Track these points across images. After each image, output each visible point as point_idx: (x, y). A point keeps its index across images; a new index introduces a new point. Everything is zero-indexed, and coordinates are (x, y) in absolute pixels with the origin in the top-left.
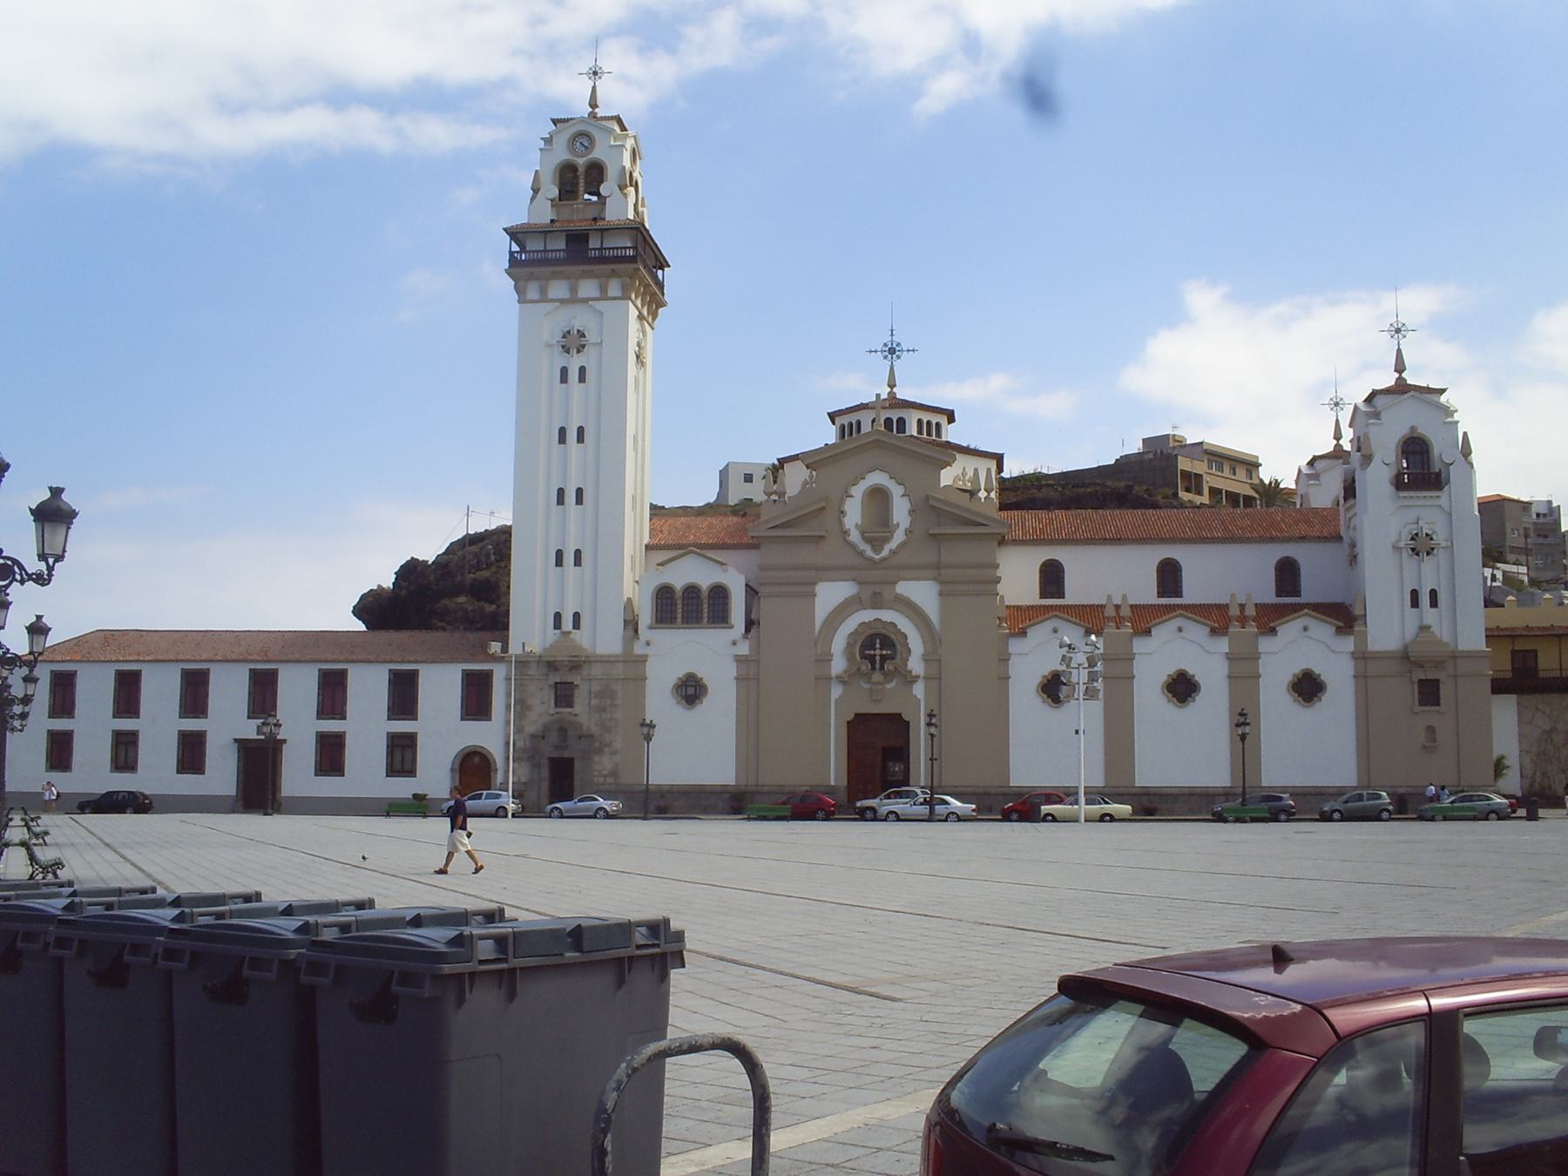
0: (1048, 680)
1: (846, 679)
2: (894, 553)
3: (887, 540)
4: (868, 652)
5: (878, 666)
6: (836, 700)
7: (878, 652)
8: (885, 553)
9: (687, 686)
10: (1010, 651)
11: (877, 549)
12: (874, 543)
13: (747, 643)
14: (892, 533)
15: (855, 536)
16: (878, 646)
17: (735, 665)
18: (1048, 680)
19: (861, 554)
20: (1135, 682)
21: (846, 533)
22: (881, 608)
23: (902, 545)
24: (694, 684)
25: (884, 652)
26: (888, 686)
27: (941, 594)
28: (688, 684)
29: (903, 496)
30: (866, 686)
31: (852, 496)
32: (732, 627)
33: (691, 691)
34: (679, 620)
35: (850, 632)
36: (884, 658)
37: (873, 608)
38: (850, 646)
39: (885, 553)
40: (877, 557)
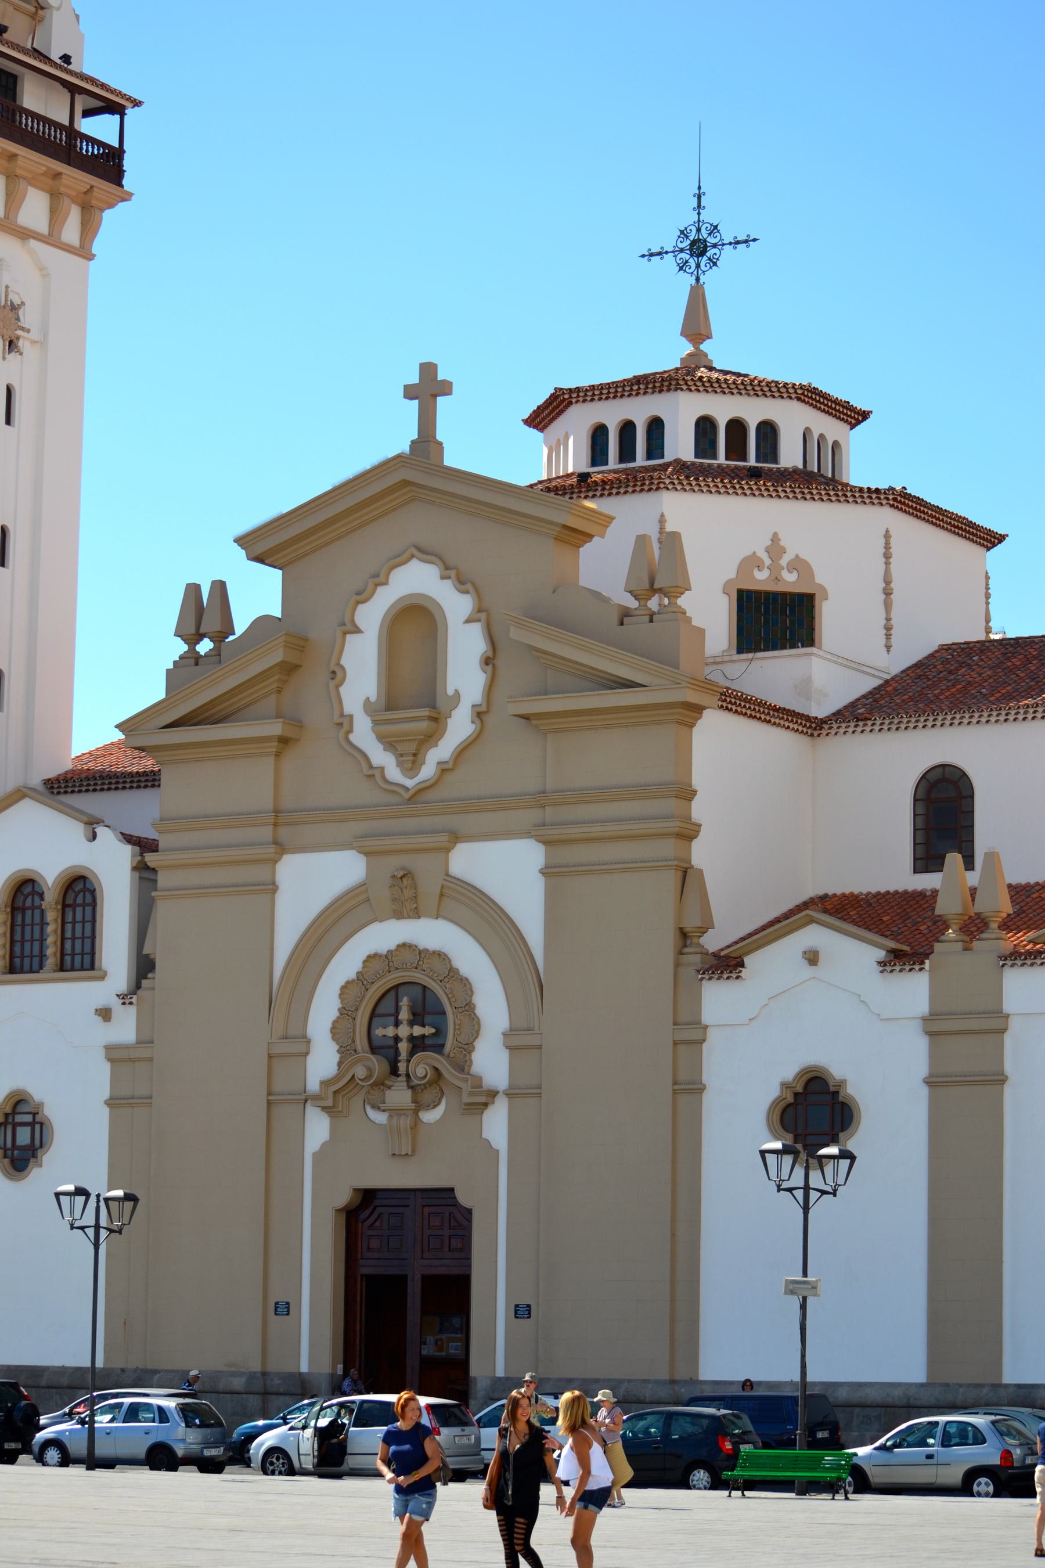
0: (796, 1095)
1: (329, 1102)
2: (443, 770)
3: (431, 738)
4: (429, 1030)
5: (402, 1067)
6: (315, 1155)
7: (404, 1031)
8: (428, 771)
9: (15, 1125)
10: (707, 1018)
11: (412, 762)
12: (401, 748)
13: (132, 1010)
14: (438, 721)
15: (363, 734)
16: (404, 1015)
17: (105, 1069)
18: (796, 1095)
19: (374, 774)
20: (1008, 1090)
21: (345, 724)
22: (416, 914)
23: (463, 751)
24: (28, 1118)
25: (418, 1031)
26: (430, 1117)
27: (547, 872)
28: (19, 1118)
29: (468, 621)
30: (379, 1117)
31: (358, 631)
32: (102, 977)
33: (24, 1136)
34: (51, 961)
35: (343, 983)
36: (418, 1044)
37: (399, 915)
38: (346, 1013)
39: (428, 771)
40: (409, 783)
